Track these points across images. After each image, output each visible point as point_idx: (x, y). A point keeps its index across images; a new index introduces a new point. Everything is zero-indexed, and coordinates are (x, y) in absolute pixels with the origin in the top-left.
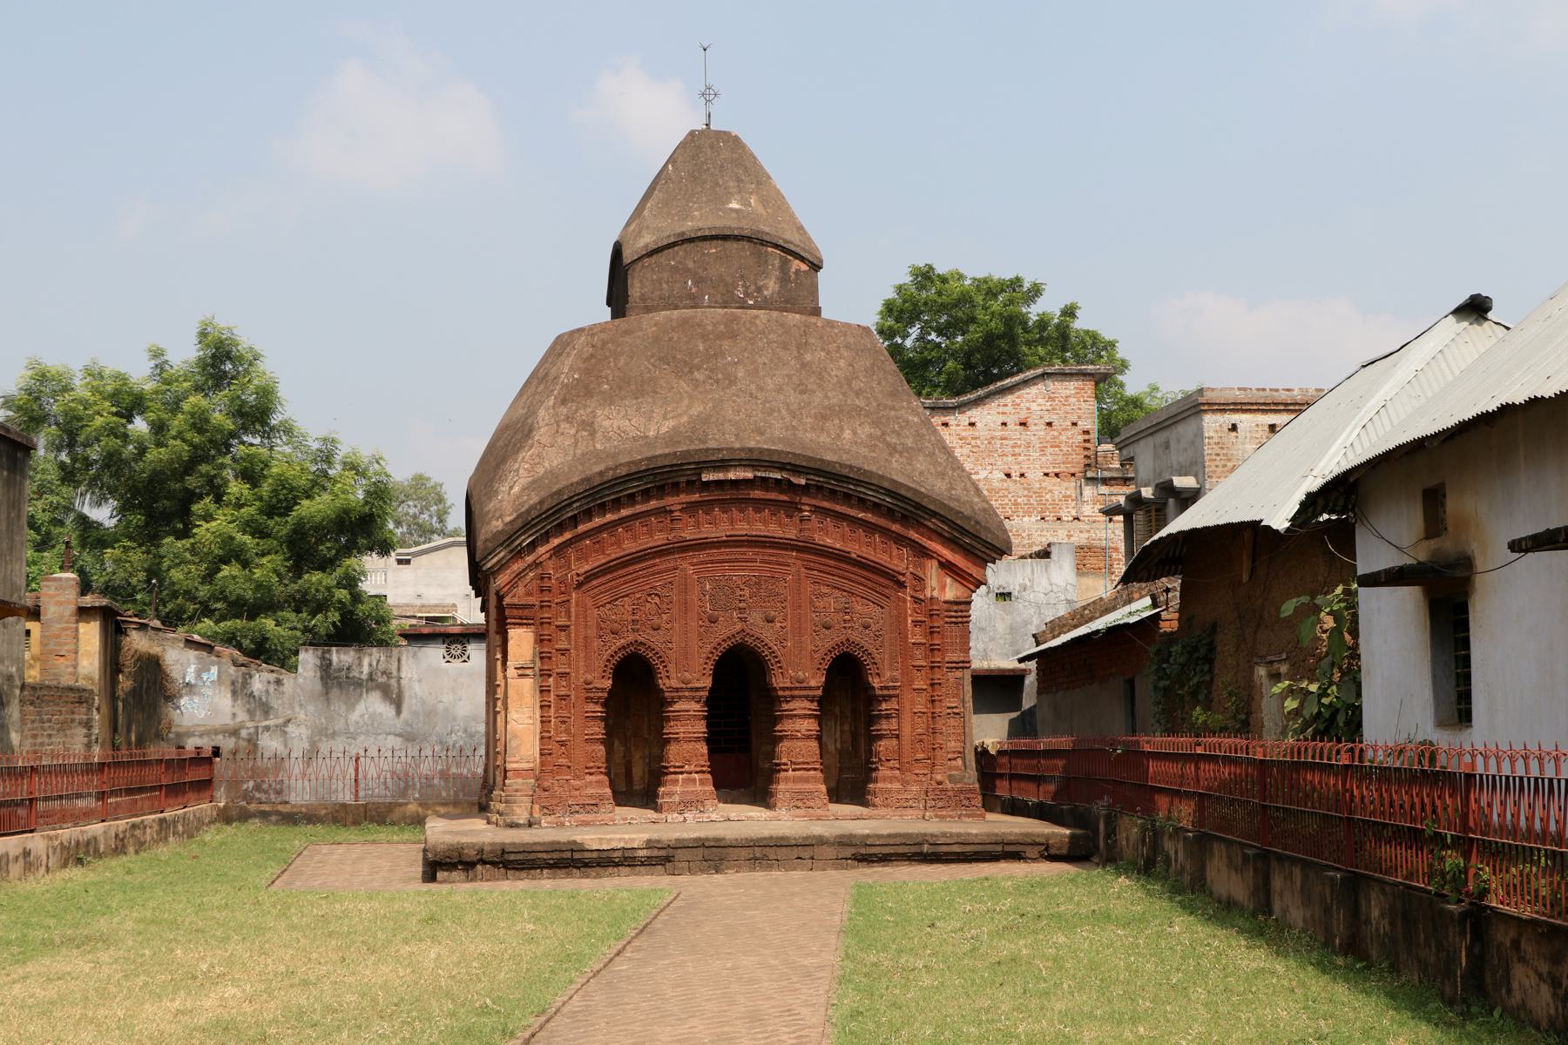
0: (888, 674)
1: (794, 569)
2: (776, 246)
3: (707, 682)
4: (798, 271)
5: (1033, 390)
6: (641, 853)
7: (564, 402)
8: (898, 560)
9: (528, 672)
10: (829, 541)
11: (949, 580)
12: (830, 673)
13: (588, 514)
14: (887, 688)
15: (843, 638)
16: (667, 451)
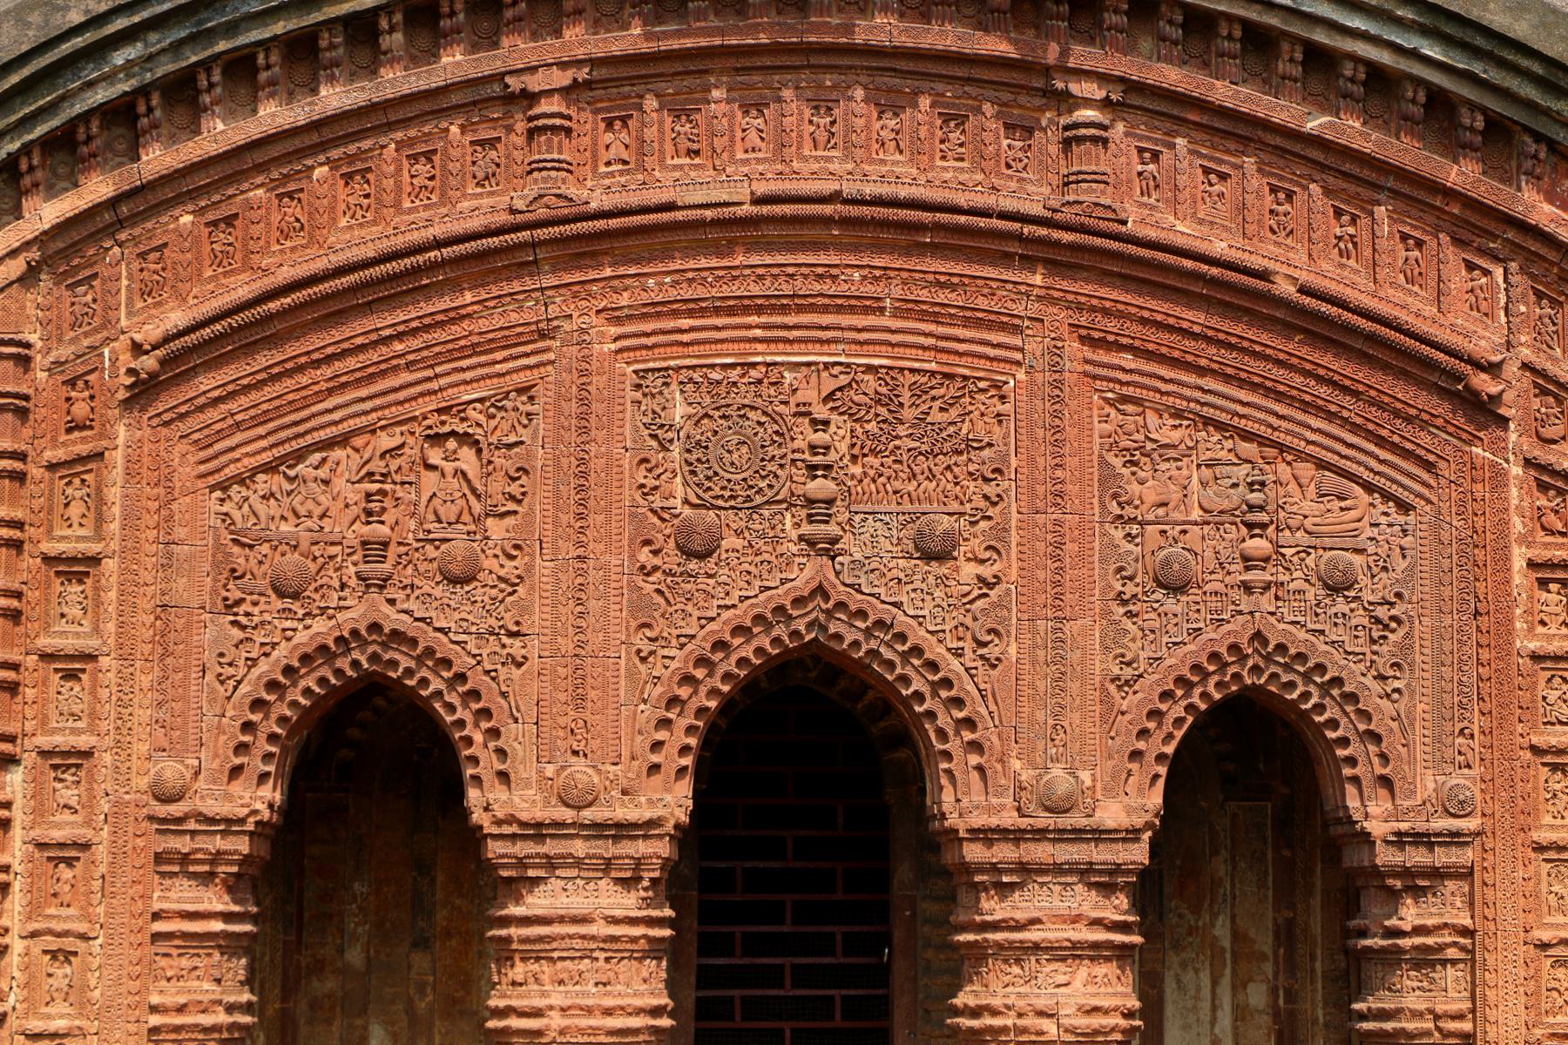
10: (1183, 231)
12: (1186, 775)
14: (1424, 840)
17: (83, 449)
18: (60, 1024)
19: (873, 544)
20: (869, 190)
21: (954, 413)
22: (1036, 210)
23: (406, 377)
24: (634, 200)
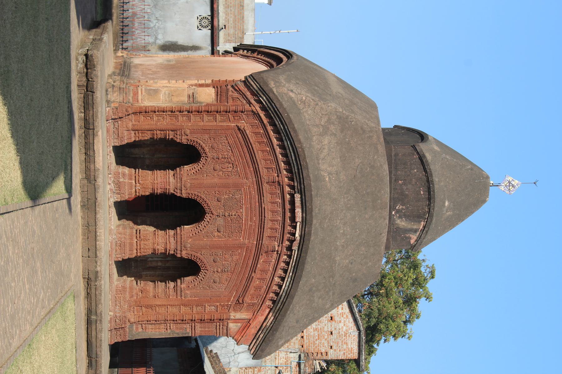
0: (188, 292)
2: (424, 227)
3: (184, 196)
4: (410, 238)
5: (351, 324)
6: (92, 166)
7: (339, 118)
9: (191, 99)
10: (261, 261)
15: (208, 268)
16: (311, 176)
20: (266, 221)
24: (264, 191)
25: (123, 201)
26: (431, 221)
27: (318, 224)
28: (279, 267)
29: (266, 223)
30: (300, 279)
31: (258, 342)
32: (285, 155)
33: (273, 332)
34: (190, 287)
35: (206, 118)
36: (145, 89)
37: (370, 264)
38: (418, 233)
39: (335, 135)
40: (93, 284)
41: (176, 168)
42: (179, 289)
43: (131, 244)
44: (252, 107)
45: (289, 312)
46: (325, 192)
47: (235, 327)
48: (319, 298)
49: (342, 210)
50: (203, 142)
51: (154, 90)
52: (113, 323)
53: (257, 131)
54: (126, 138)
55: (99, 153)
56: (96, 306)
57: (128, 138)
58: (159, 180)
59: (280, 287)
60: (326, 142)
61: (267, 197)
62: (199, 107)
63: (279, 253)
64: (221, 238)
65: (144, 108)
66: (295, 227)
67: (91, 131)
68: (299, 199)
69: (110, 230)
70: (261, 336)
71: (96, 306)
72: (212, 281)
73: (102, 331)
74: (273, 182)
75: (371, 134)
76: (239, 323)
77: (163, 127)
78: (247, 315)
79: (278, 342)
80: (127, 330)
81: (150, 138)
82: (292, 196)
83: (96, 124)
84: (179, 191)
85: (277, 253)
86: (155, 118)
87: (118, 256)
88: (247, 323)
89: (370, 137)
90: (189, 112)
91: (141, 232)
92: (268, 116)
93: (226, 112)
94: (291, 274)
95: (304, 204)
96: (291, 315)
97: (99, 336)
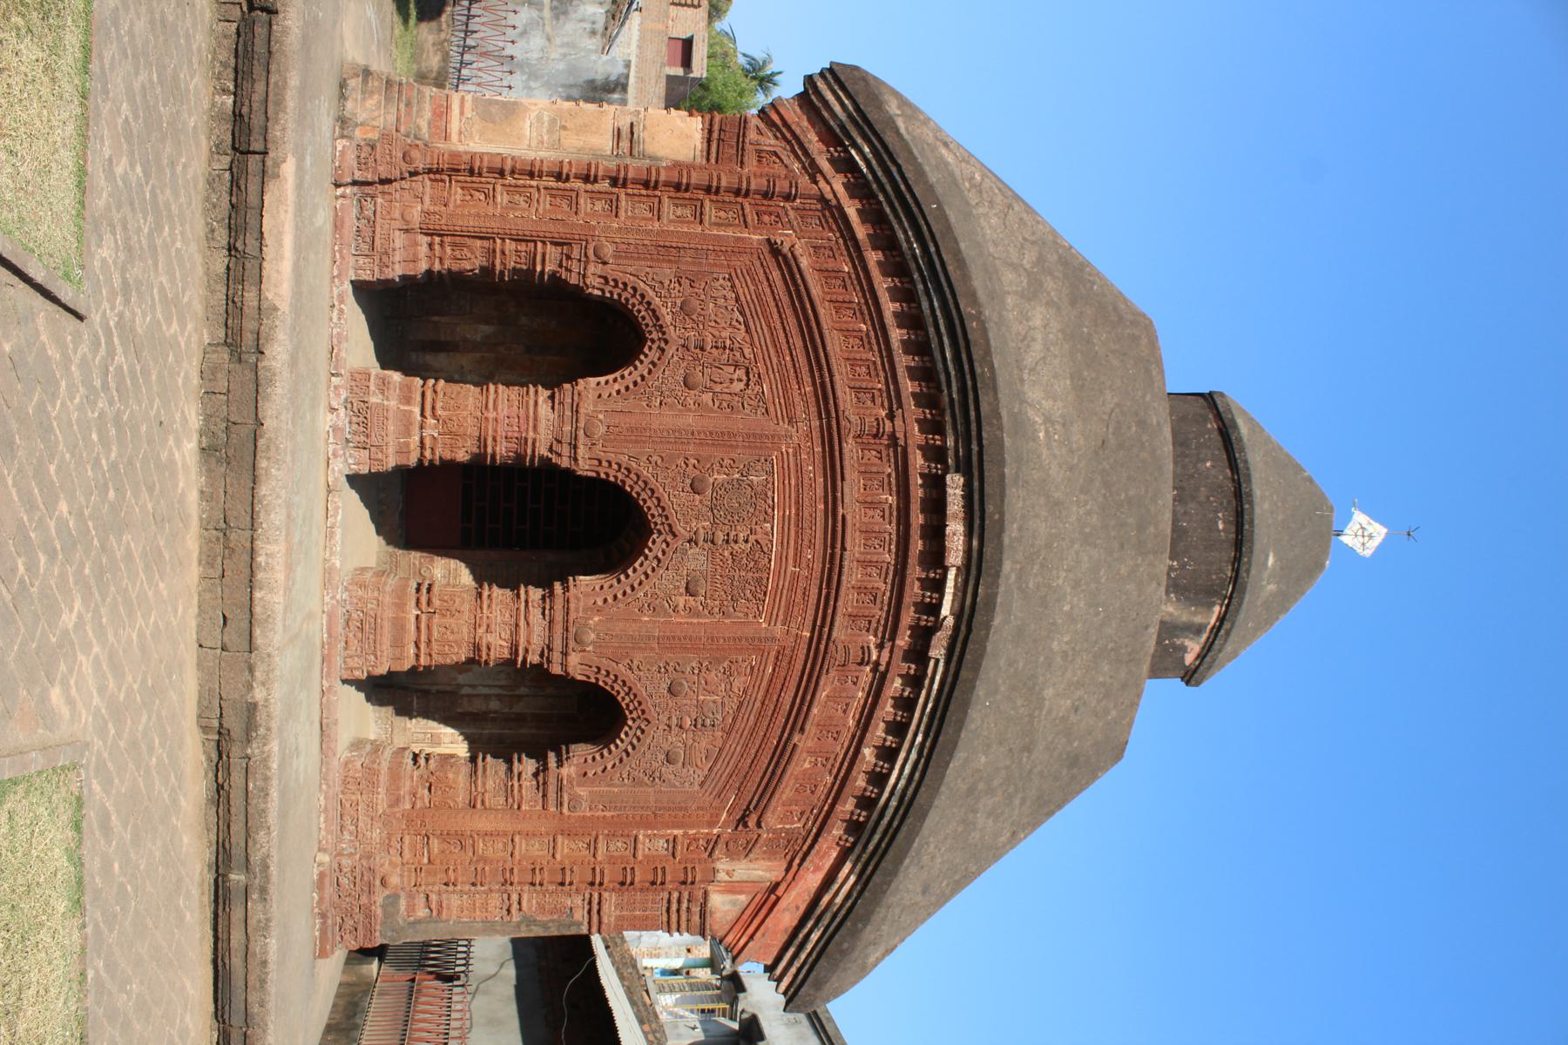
0: (582, 792)
1: (779, 630)
2: (1222, 619)
3: (584, 468)
4: (1184, 649)
6: (250, 297)
8: (782, 817)
9: (625, 144)
10: (823, 694)
11: (743, 899)
13: (897, 266)
14: (560, 789)
15: (652, 714)
16: (1004, 413)
17: (749, 219)
18: (499, 199)
19: (697, 560)
20: (846, 563)
21: (749, 595)
22: (834, 635)
23: (775, 360)
25: (378, 474)
26: (1240, 604)
27: (1013, 576)
28: (878, 714)
29: (845, 570)
30: (951, 755)
31: (803, 956)
32: (918, 347)
33: (855, 925)
34: (590, 774)
35: (668, 207)
36: (475, 100)
37: (1114, 713)
38: (1204, 636)
39: (1059, 309)
40: (236, 751)
41: (559, 385)
42: (552, 781)
43: (399, 625)
44: (822, 184)
45: (907, 861)
46: (1036, 475)
47: (727, 907)
48: (989, 815)
49: (1073, 542)
50: (656, 291)
51: (504, 105)
52: (329, 890)
53: (831, 265)
54: (397, 258)
55: (280, 244)
56: (248, 836)
57: (407, 258)
58: (503, 409)
59: (878, 779)
60: (1037, 322)
61: (852, 488)
62: (649, 170)
63: (882, 668)
64: (698, 615)
65: (466, 158)
66: (938, 586)
67: (254, 161)
68: (959, 492)
69: (329, 572)
70: (815, 937)
71: (248, 836)
72: (662, 757)
73: (267, 928)
74: (875, 436)
75: (1137, 332)
76: (741, 893)
77: (527, 228)
78: (769, 870)
79: (867, 956)
80: (379, 911)
81: (482, 268)
82: (936, 485)
83: (275, 132)
84: (566, 450)
85: (875, 670)
86: (502, 198)
87: (351, 663)
88: (770, 896)
89: (1135, 339)
90: (614, 182)
91: (436, 589)
92: (873, 215)
93: (737, 193)
94: (919, 738)
95: (976, 507)
96: (913, 870)
97: (256, 947)
